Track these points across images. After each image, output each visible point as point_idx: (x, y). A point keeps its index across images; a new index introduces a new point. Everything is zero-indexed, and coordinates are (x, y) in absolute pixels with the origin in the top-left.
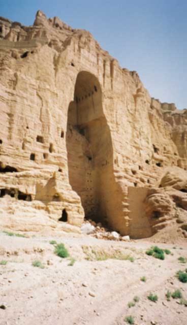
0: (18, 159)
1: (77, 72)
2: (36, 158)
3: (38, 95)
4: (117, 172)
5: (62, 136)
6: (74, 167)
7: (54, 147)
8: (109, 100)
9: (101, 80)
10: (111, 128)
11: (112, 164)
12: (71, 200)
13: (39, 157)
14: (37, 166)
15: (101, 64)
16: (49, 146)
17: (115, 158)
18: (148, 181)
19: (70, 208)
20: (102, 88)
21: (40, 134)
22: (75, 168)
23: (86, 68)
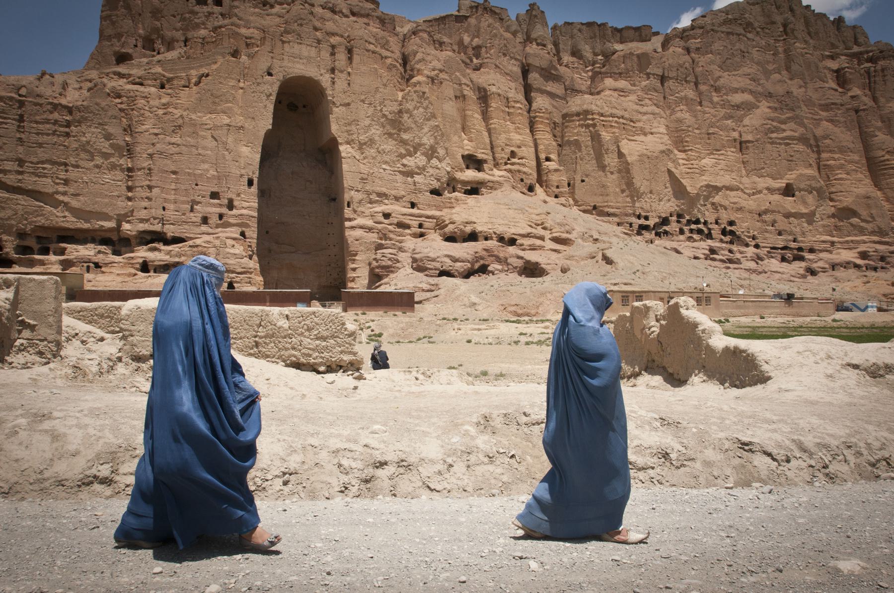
0: (186, 227)
1: (278, 83)
2: (210, 221)
3: (212, 137)
4: (350, 220)
5: (250, 183)
7: (236, 203)
8: (343, 109)
9: (325, 80)
10: (343, 155)
11: (343, 209)
12: (240, 270)
13: (214, 220)
14: (210, 231)
15: (325, 54)
16: (226, 201)
17: (347, 197)
18: (421, 226)
19: (238, 279)
20: (329, 92)
21: (215, 189)
23: (296, 71)
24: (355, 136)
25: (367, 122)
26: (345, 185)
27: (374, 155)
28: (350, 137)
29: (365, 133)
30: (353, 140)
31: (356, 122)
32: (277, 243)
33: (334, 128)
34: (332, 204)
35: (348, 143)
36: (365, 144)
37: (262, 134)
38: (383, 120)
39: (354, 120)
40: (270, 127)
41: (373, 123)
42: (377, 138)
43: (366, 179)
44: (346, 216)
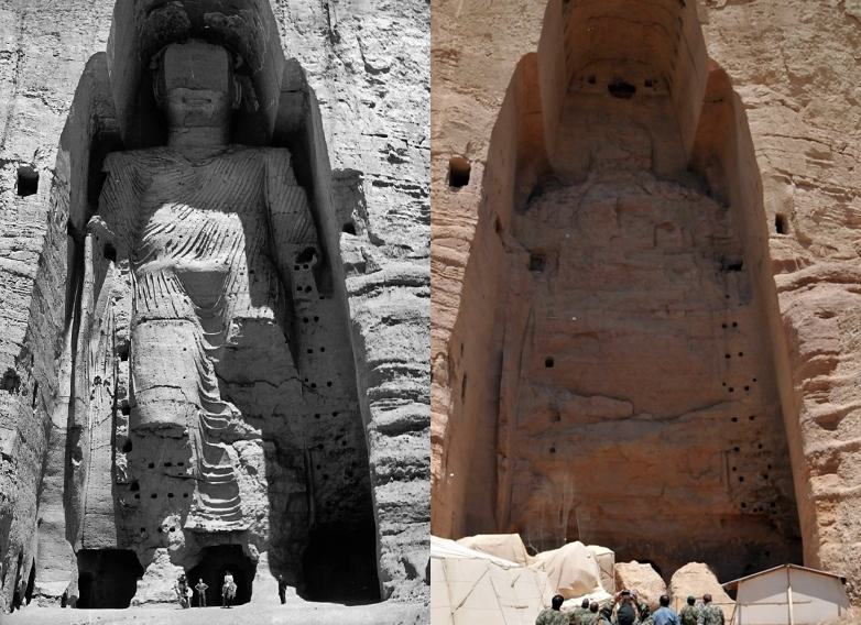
4: (790, 266)
6: (653, 311)
22: (661, 314)
24: (776, 65)
25: (807, 33)
26: (763, 169)
27: (840, 108)
28: (764, 68)
29: (805, 56)
30: (772, 74)
31: (778, 32)
32: (576, 392)
33: (715, 50)
34: (732, 275)
35: (758, 80)
36: (809, 79)
37: (509, 65)
38: (847, 29)
39: (770, 29)
40: (534, 49)
41: (824, 35)
42: (839, 69)
43: (828, 156)
44: (776, 255)
